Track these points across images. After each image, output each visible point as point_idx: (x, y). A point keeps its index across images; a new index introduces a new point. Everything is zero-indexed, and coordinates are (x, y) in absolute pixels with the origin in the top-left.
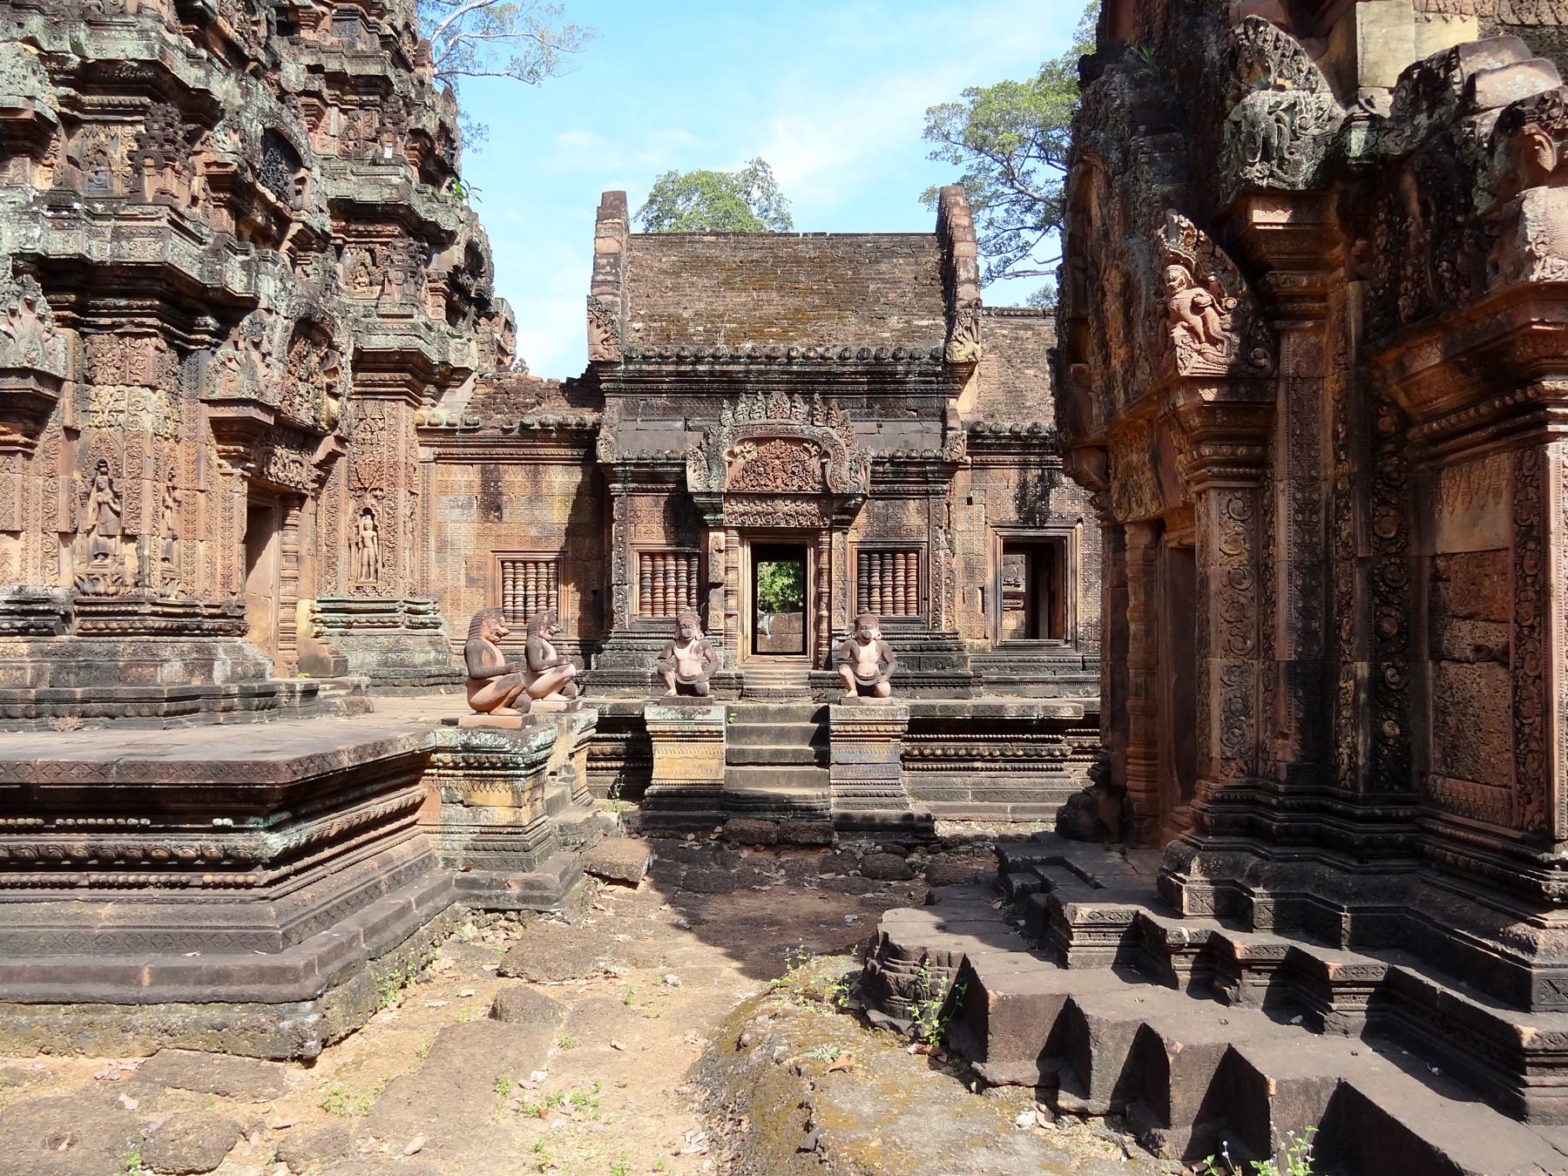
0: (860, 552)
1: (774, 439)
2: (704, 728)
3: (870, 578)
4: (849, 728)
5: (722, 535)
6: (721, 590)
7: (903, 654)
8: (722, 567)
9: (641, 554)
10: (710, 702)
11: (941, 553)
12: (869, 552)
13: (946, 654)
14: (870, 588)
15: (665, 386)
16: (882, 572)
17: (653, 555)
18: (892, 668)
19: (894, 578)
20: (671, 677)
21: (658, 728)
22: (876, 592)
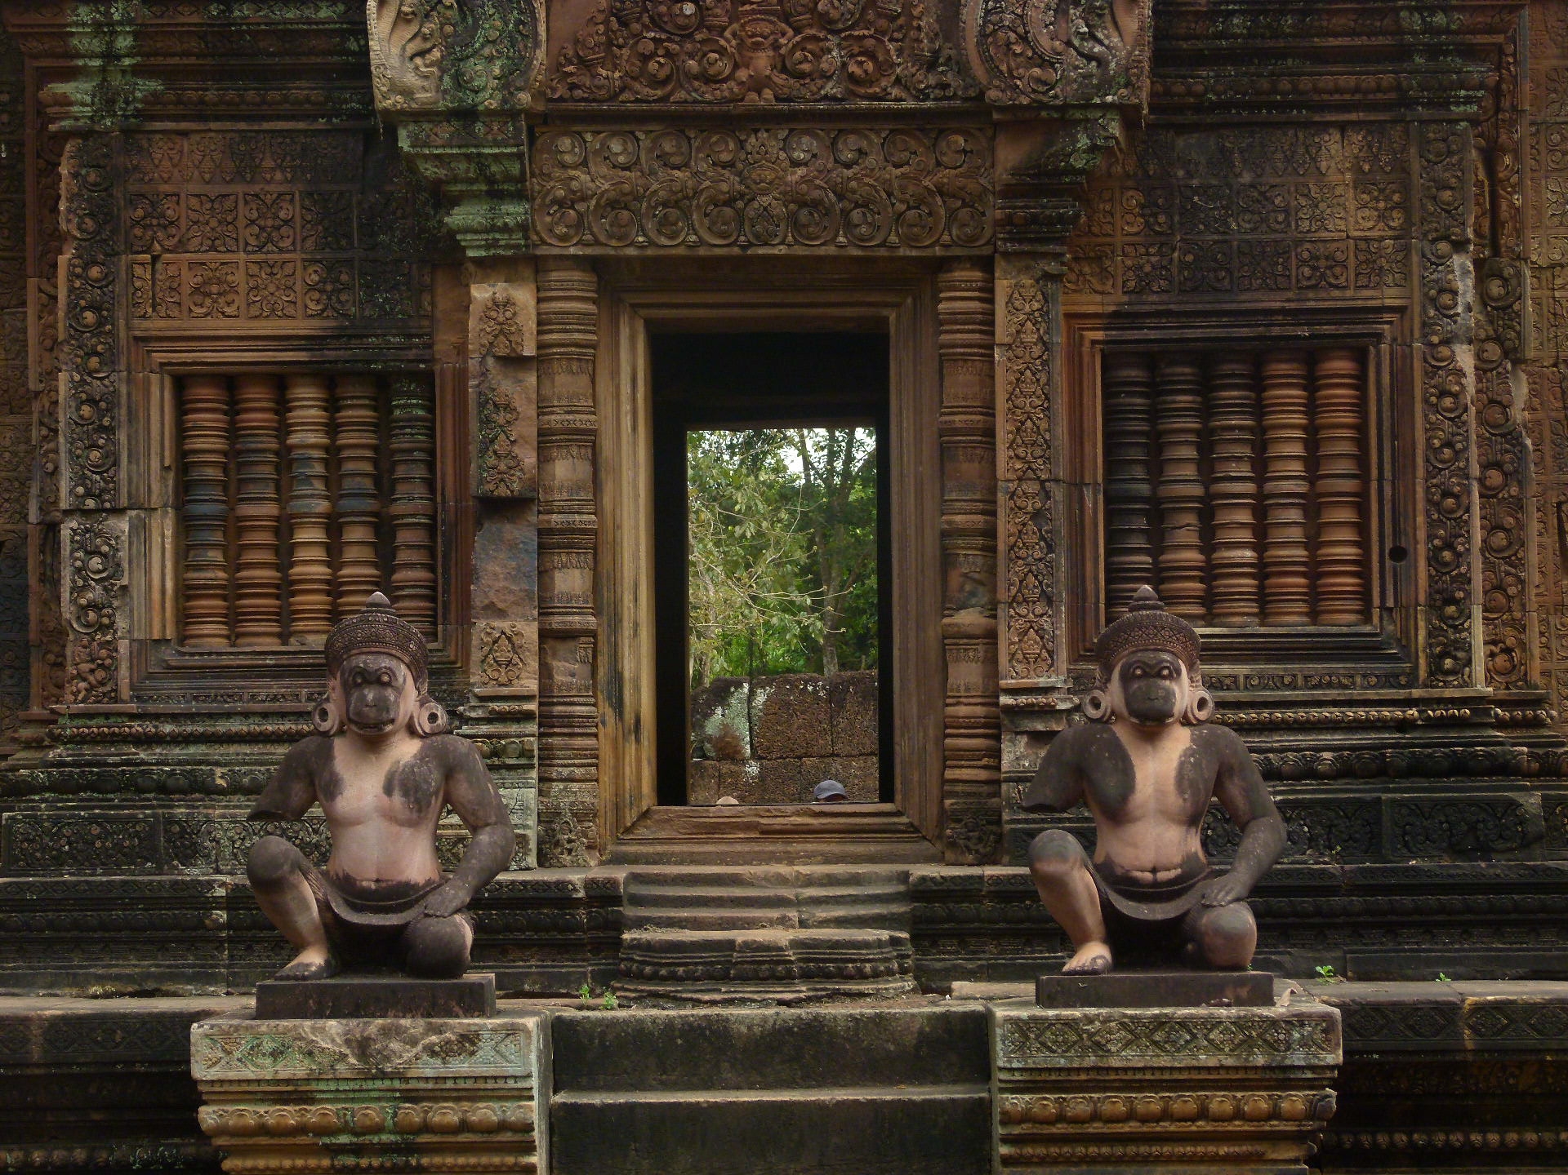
0: (1111, 359)
2: (448, 1114)
3: (1156, 467)
4: (1079, 1104)
5: (524, 296)
6: (522, 533)
7: (1307, 791)
8: (526, 428)
9: (181, 383)
10: (475, 1002)
11: (1465, 358)
12: (1152, 358)
13: (1483, 790)
14: (1159, 513)
16: (1206, 444)
17: (230, 382)
18: (1263, 842)
19: (1261, 466)
20: (308, 896)
21: (252, 1114)
22: (1185, 532)
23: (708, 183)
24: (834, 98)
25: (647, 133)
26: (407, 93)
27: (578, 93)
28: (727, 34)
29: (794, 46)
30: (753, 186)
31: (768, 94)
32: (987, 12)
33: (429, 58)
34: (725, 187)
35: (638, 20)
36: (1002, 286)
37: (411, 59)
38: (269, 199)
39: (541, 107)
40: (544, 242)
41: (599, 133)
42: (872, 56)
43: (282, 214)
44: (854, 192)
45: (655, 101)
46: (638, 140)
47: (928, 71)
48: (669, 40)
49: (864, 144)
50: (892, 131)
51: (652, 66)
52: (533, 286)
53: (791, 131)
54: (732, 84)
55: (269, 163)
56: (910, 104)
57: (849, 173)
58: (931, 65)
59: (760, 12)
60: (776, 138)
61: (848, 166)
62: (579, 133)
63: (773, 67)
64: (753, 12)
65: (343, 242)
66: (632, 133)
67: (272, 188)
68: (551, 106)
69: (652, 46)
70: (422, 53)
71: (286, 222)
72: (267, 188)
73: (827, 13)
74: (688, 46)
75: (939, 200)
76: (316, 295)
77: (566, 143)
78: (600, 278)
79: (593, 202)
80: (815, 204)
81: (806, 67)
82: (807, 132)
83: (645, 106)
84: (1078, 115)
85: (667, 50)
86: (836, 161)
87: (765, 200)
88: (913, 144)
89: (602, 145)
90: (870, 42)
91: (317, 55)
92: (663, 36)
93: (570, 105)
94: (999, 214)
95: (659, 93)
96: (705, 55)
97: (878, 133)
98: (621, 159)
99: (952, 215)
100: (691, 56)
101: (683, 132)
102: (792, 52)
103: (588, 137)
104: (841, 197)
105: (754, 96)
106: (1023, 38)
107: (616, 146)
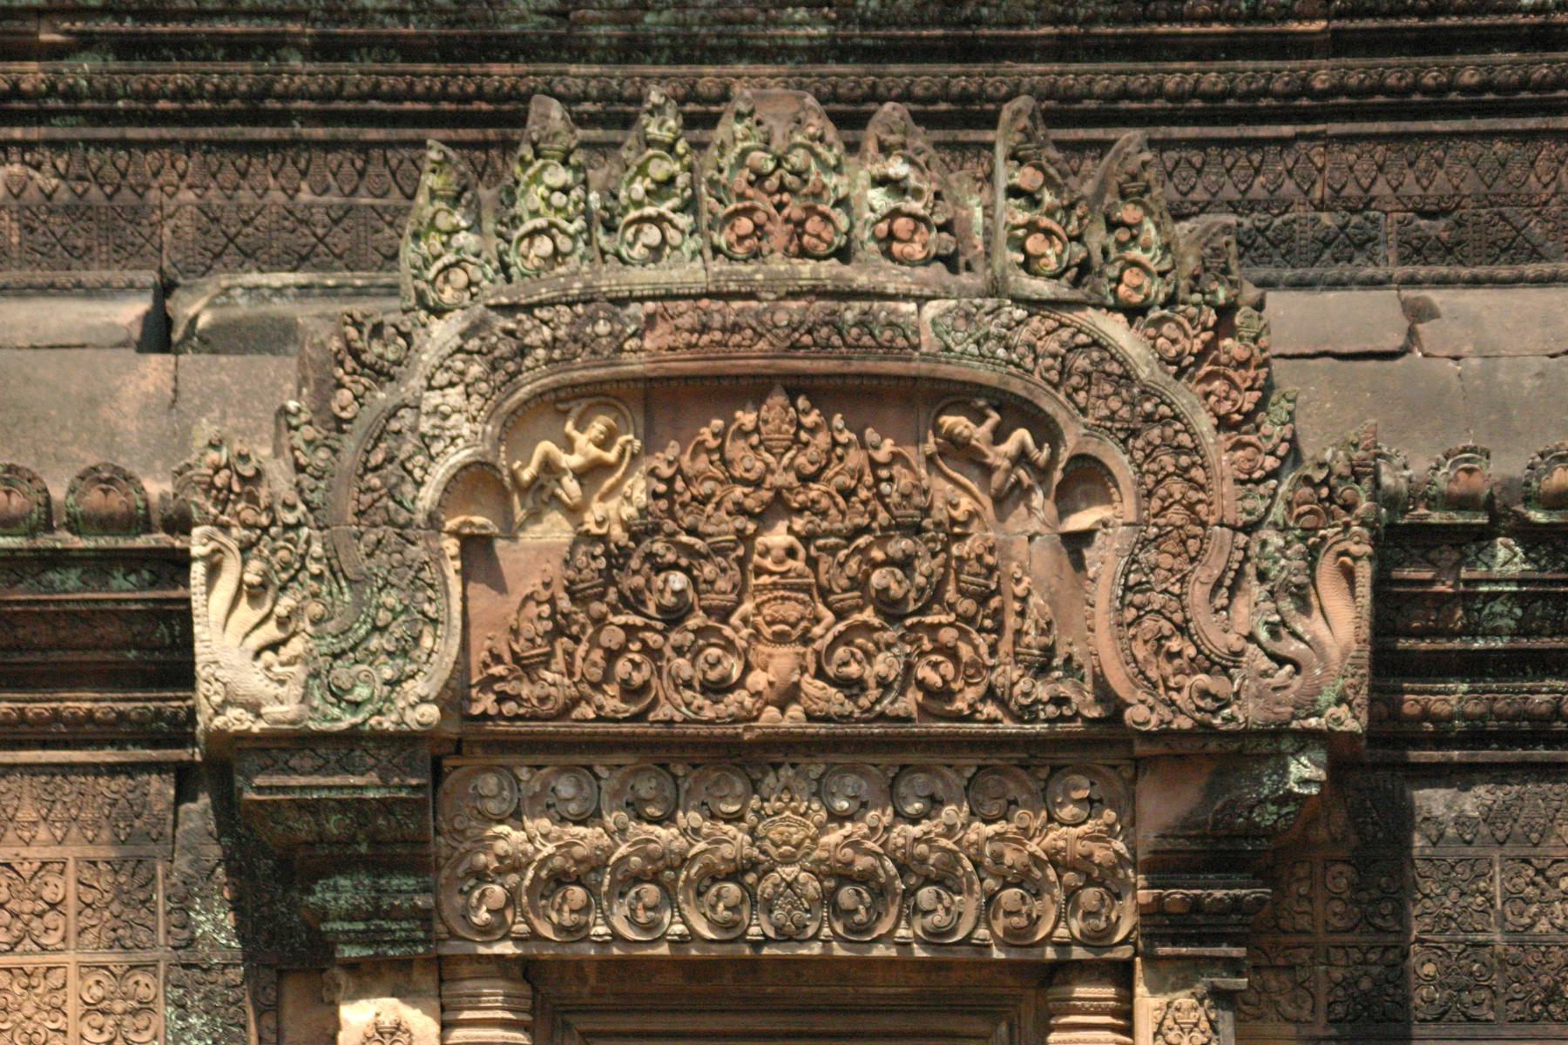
1: (753, 389)
15: (32, 74)
23: (701, 845)
24: (897, 719)
25: (610, 768)
26: (254, 708)
27: (509, 708)
28: (735, 620)
29: (835, 638)
30: (772, 850)
31: (795, 710)
32: (1127, 588)
33: (286, 652)
34: (727, 850)
35: (601, 597)
36: (1147, 1004)
37: (257, 655)
38: (26, 870)
39: (453, 729)
40: (453, 935)
41: (539, 767)
42: (952, 654)
43: (48, 894)
44: (923, 860)
45: (625, 720)
46: (597, 777)
47: (1036, 677)
48: (647, 628)
49: (939, 788)
50: (980, 768)
51: (622, 667)
52: (436, 1004)
53: (830, 766)
54: (742, 695)
55: (27, 814)
56: (1009, 727)
57: (916, 831)
58: (1042, 669)
59: (784, 587)
60: (807, 777)
61: (915, 820)
62: (510, 769)
63: (804, 670)
64: (775, 586)
65: (143, 936)
66: (589, 768)
67: (33, 852)
68: (470, 727)
69: (621, 635)
70: (274, 646)
71: (53, 906)
72: (24, 852)
73: (886, 589)
74: (675, 637)
75: (1051, 873)
76: (99, 1019)
77: (490, 783)
78: (535, 989)
79: (530, 873)
80: (865, 879)
81: (853, 670)
82: (852, 769)
83: (612, 728)
84: (1265, 747)
85: (644, 642)
86: (897, 814)
87: (789, 872)
88: (1013, 791)
89: (544, 786)
90: (947, 636)
91: (106, 649)
92: (639, 621)
93: (503, 726)
94: (1144, 896)
95: (633, 709)
96: (701, 650)
97: (959, 771)
98: (573, 808)
99: (1072, 894)
100: (679, 651)
101: (664, 766)
102: (832, 647)
103: (524, 774)
104: (903, 869)
105: (772, 711)
106: (1182, 629)
107: (565, 788)
